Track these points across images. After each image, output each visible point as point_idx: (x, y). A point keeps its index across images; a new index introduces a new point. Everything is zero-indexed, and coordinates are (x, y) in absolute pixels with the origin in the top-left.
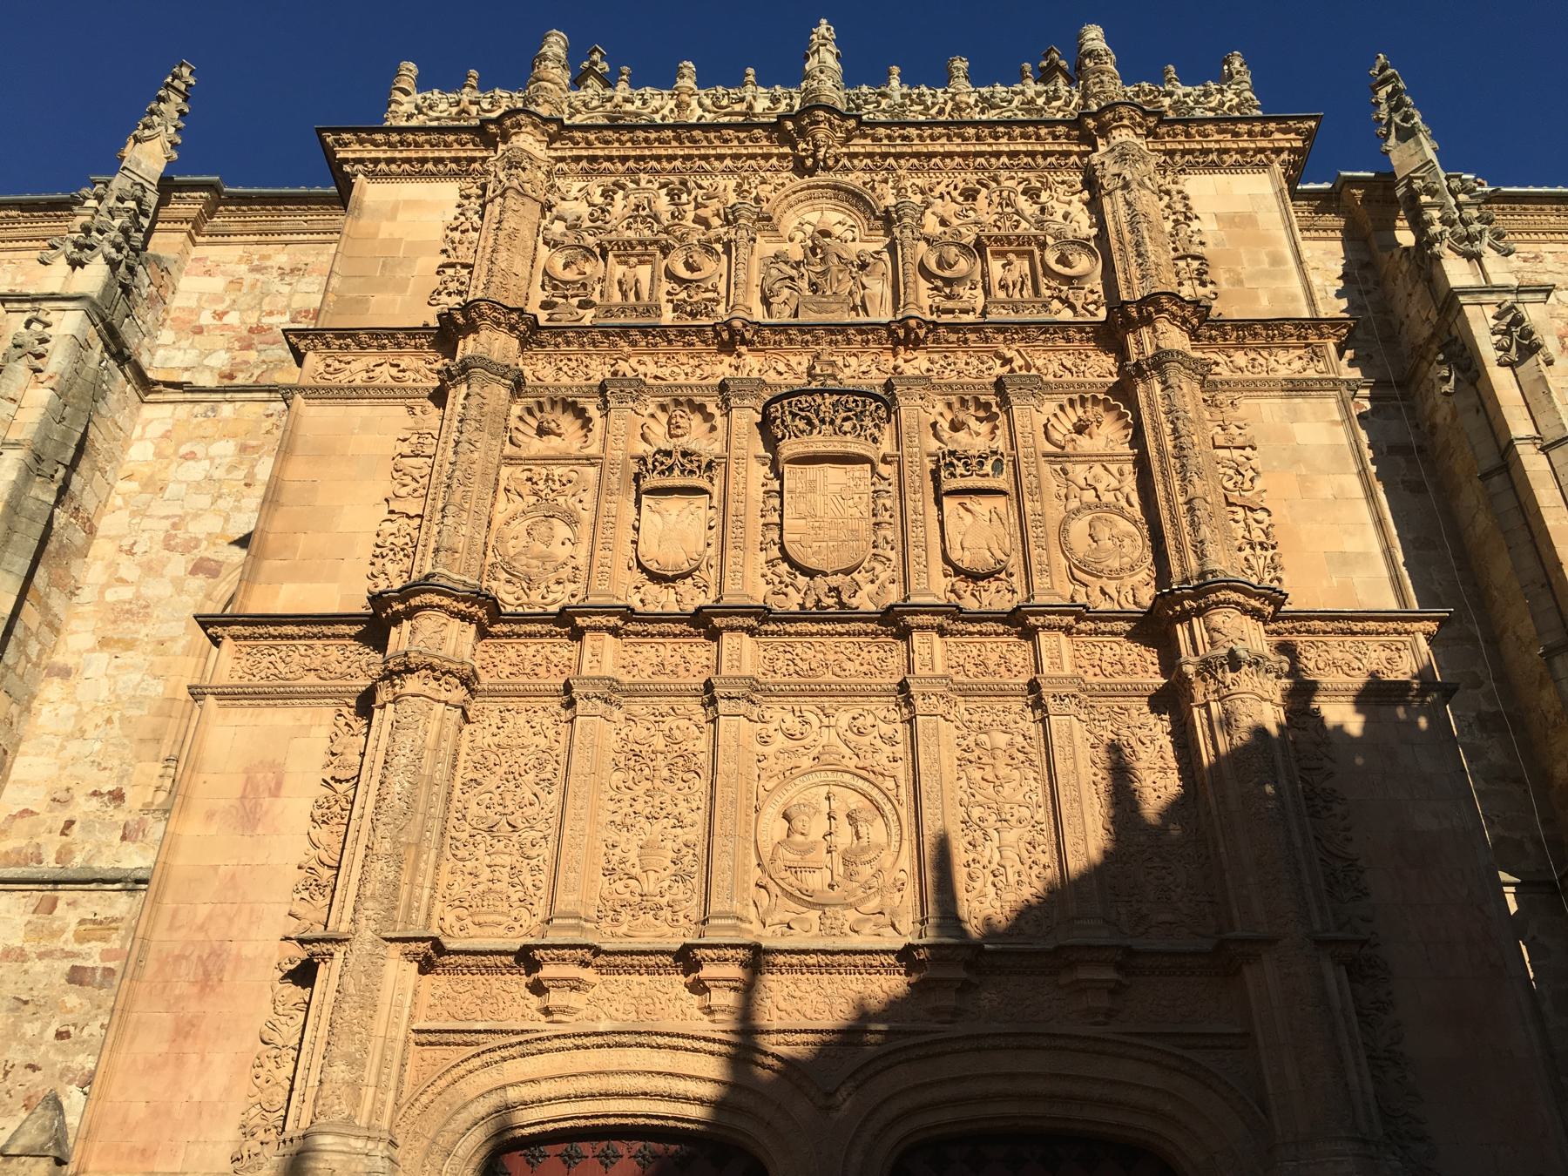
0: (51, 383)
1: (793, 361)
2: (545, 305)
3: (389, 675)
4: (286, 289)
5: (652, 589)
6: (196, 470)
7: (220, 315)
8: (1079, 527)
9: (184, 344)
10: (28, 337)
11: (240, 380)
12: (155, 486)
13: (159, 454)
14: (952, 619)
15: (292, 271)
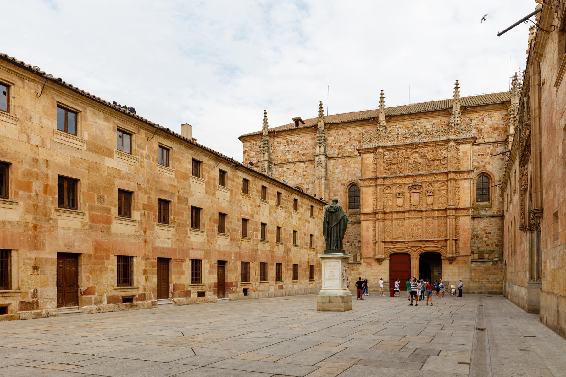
0: (324, 168)
1: (412, 178)
2: (385, 172)
3: (377, 220)
4: (342, 138)
5: (399, 208)
6: (338, 170)
7: (335, 144)
8: (440, 198)
9: (331, 149)
10: (319, 162)
11: (340, 155)
12: (334, 173)
13: (333, 168)
14: (426, 211)
15: (343, 134)
